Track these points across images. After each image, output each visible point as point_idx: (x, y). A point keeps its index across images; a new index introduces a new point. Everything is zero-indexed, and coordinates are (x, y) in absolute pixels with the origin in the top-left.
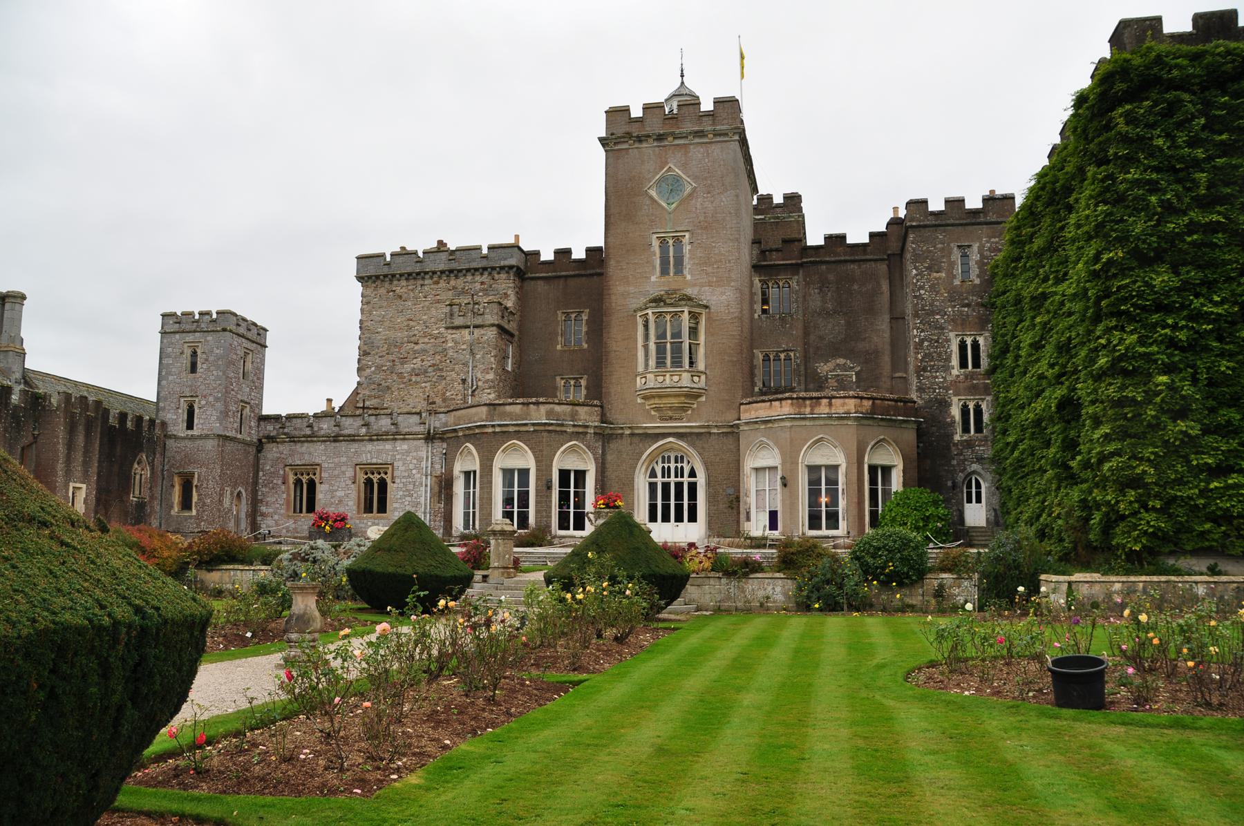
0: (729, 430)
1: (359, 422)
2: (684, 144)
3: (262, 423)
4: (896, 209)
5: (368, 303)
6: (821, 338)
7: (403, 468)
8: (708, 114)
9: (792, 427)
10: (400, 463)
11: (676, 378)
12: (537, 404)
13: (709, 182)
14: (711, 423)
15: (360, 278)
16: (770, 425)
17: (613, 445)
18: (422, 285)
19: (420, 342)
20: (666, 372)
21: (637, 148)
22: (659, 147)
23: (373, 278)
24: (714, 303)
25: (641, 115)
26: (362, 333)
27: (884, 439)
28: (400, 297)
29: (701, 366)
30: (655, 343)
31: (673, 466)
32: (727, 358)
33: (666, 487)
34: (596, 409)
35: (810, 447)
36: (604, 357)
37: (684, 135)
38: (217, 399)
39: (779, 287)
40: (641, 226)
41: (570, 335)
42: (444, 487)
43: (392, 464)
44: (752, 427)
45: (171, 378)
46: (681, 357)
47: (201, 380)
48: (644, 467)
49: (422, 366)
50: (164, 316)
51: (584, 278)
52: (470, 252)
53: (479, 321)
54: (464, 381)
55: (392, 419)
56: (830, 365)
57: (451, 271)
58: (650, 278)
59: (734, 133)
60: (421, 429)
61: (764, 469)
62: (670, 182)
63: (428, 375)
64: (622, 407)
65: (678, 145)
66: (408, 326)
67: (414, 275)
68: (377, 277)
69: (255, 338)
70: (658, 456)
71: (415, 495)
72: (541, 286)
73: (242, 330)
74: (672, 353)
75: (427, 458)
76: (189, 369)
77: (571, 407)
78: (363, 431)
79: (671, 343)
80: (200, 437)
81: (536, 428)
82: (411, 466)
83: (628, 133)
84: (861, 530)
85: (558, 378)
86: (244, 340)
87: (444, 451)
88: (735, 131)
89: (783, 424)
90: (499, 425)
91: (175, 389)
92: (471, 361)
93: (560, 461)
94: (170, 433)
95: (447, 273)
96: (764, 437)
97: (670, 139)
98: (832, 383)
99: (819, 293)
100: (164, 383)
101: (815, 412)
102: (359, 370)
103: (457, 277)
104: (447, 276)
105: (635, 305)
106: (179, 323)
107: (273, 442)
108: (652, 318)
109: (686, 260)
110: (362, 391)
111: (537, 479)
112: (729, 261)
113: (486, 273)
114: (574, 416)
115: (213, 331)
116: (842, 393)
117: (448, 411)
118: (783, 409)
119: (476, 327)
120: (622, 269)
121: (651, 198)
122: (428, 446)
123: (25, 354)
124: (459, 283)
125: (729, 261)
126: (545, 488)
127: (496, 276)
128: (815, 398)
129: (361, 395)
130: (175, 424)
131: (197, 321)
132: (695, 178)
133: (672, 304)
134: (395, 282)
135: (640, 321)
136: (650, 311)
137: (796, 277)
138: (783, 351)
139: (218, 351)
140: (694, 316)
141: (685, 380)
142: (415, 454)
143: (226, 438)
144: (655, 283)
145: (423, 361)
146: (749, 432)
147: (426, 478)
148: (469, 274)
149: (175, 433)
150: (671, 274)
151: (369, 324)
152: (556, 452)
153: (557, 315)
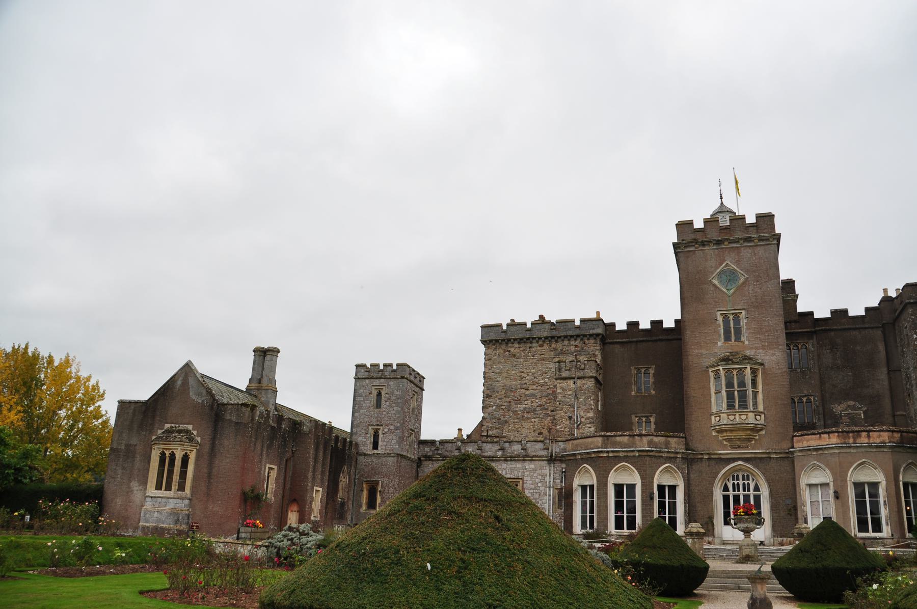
1: (497, 447)
2: (736, 247)
3: (421, 446)
4: (885, 290)
5: (490, 359)
8: (752, 225)
10: (529, 478)
11: (744, 417)
12: (641, 435)
15: (484, 342)
16: (821, 452)
17: (695, 467)
20: (736, 412)
21: (701, 250)
22: (717, 249)
24: (767, 361)
25: (703, 227)
26: (486, 382)
27: (912, 462)
28: (514, 356)
29: (761, 408)
31: (741, 482)
33: (736, 499)
34: (683, 440)
35: (855, 469)
36: (685, 401)
38: (397, 428)
39: (798, 349)
41: (641, 385)
42: (565, 498)
44: (805, 453)
45: (362, 411)
46: (746, 401)
47: (385, 413)
48: (720, 483)
49: (532, 406)
50: (357, 366)
52: (567, 324)
53: (581, 374)
54: (570, 418)
55: (521, 445)
56: (843, 406)
57: (553, 337)
58: (717, 343)
59: (774, 239)
60: (545, 453)
61: (816, 485)
62: (728, 274)
63: (537, 412)
64: (701, 438)
65: (732, 248)
66: (520, 376)
67: (525, 340)
68: (497, 341)
69: (418, 383)
70: (730, 475)
72: (618, 349)
73: (412, 378)
74: (739, 398)
75: (550, 474)
76: (375, 405)
78: (500, 453)
79: (738, 391)
80: (384, 455)
81: (641, 454)
82: (537, 481)
83: (695, 240)
85: (633, 416)
87: (564, 470)
89: (832, 451)
90: (612, 451)
91: (365, 420)
92: (576, 403)
94: (361, 451)
95: (550, 338)
96: (816, 461)
97: (726, 243)
98: (846, 420)
99: (830, 353)
100: (356, 414)
101: (857, 442)
102: (483, 408)
103: (557, 342)
104: (550, 341)
105: (707, 363)
106: (369, 372)
107: (430, 460)
108: (722, 373)
109: (744, 330)
111: (643, 492)
112: (777, 331)
113: (578, 341)
114: (667, 445)
115: (394, 378)
117: (567, 440)
118: (831, 440)
119: (579, 378)
121: (715, 286)
122: (551, 466)
123: (277, 391)
124: (559, 346)
126: (648, 498)
127: (587, 341)
128: (856, 431)
129: (485, 427)
130: (365, 444)
131: (382, 371)
132: (747, 271)
133: (738, 362)
134: (510, 345)
135: (712, 375)
136: (721, 368)
137: (811, 341)
139: (398, 393)
140: (754, 372)
141: (751, 419)
142: (540, 471)
144: (721, 347)
145: (532, 402)
146: (803, 457)
147: (549, 490)
148: (566, 339)
149: (365, 451)
150: (733, 340)
152: (655, 472)
153: (631, 369)
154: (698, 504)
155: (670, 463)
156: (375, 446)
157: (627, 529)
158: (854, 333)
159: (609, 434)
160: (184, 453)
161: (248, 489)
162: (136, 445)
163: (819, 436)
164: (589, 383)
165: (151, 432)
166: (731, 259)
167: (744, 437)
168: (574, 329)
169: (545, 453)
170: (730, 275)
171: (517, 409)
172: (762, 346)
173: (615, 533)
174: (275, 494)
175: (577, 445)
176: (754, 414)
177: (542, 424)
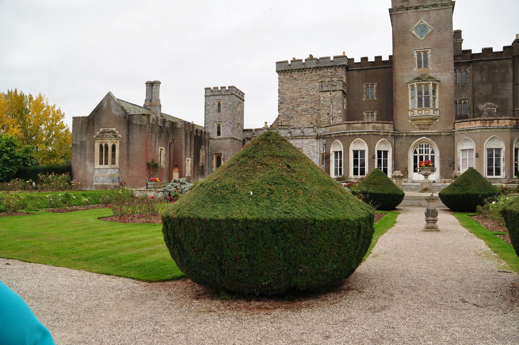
0: (449, 134)
1: (287, 131)
2: (428, 10)
3: (244, 132)
5: (281, 82)
6: (481, 94)
7: (307, 150)
9: (480, 132)
10: (305, 148)
11: (427, 112)
12: (368, 123)
13: (439, 27)
14: (441, 131)
15: (278, 72)
16: (470, 131)
17: (399, 140)
18: (305, 74)
19: (305, 98)
21: (406, 13)
22: (416, 12)
23: (284, 71)
24: (442, 79)
26: (280, 95)
28: (296, 79)
29: (437, 107)
30: (417, 97)
31: (424, 149)
32: (448, 103)
33: (421, 158)
34: (392, 125)
35: (489, 141)
36: (394, 103)
37: (428, 6)
38: (230, 123)
39: (461, 72)
40: (409, 47)
42: (326, 158)
44: (461, 132)
45: (210, 114)
46: (429, 103)
48: (412, 149)
50: (206, 89)
51: (374, 70)
52: (326, 59)
53: (334, 88)
54: (328, 114)
56: (485, 105)
57: (318, 68)
59: (451, 5)
60: (314, 134)
61: (466, 150)
62: (421, 27)
64: (402, 124)
66: (299, 91)
67: (301, 69)
68: (285, 71)
69: (241, 97)
72: (355, 73)
73: (237, 94)
74: (425, 101)
75: (317, 146)
76: (217, 111)
77: (382, 124)
78: (289, 135)
79: (424, 97)
80: (224, 139)
81: (368, 133)
82: (310, 150)
83: (402, 6)
84: (511, 177)
85: (364, 112)
86: (238, 98)
87: (325, 143)
88: (451, 3)
89: (476, 131)
90: (352, 132)
91: (212, 119)
92: (331, 105)
93: (353, 147)
94: (211, 137)
95: (316, 68)
98: (486, 113)
99: (480, 74)
100: (207, 116)
101: (491, 126)
102: (279, 110)
103: (320, 70)
104: (316, 70)
105: (407, 81)
106: (212, 92)
107: (249, 140)
108: (416, 86)
109: (429, 61)
110: (280, 119)
111: (369, 155)
112: (449, 61)
113: (333, 68)
114: (383, 128)
115: (227, 95)
116: (503, 118)
117: (326, 127)
118: (476, 125)
120: (401, 65)
121: (413, 34)
124: (321, 72)
125: (449, 61)
126: (372, 158)
127: (337, 69)
128: (491, 120)
129: (280, 120)
130: (213, 133)
131: (220, 91)
132: (433, 25)
133: (425, 80)
134: (293, 73)
135: (410, 88)
136: (415, 84)
137: (469, 67)
138: (463, 100)
139: (230, 103)
140: (434, 86)
141: (431, 113)
142: (311, 144)
143: (234, 139)
144: (416, 71)
147: (317, 155)
148: (325, 69)
149: (213, 137)
150: (423, 67)
151: (282, 90)
153: (363, 85)
154: (400, 161)
155: (384, 138)
156: (219, 134)
157: (360, 175)
158: (495, 62)
159: (350, 122)
160: (113, 144)
161: (150, 161)
162: (85, 141)
164: (339, 94)
165: (93, 133)
166: (423, 18)
167: (427, 123)
168: (330, 62)
169: (314, 134)
170: (422, 28)
171: (298, 110)
172: (440, 70)
173: (353, 177)
174: (165, 164)
175: (332, 129)
176: (433, 110)
177: (312, 118)
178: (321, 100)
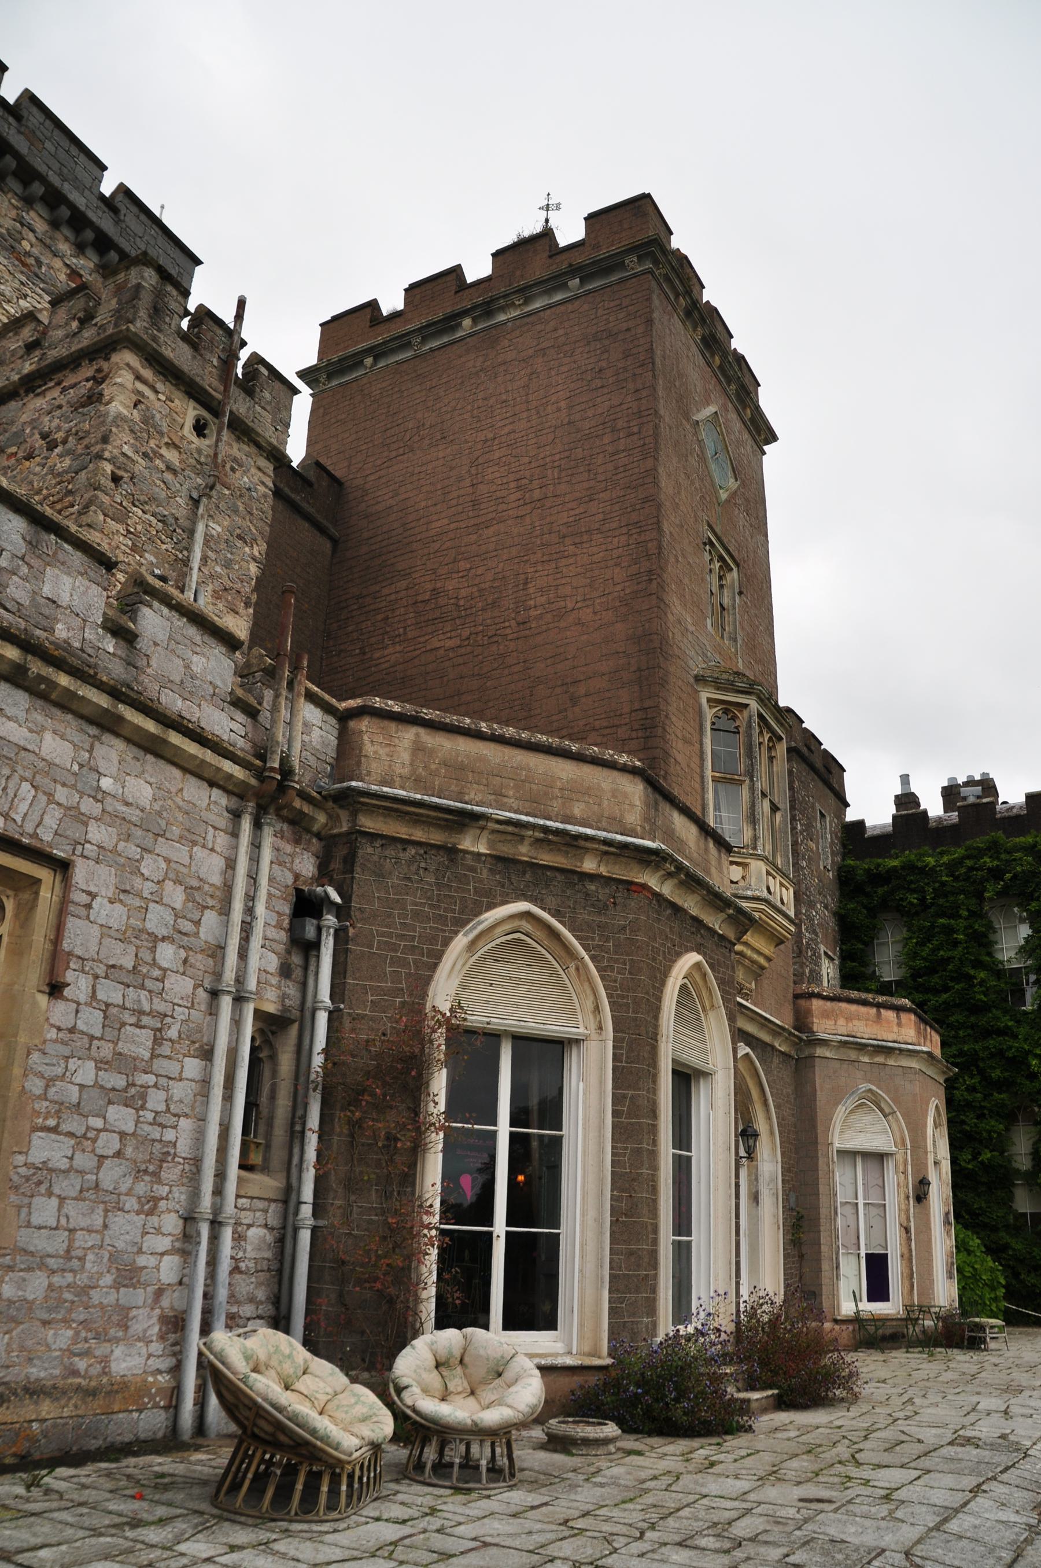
16: (880, 1059)
43: (63, 867)
71: (156, 1100)
82: (157, 920)
118: (904, 1031)
142: (180, 853)
146: (837, 1064)
163: (873, 1011)
178: (119, 418)
